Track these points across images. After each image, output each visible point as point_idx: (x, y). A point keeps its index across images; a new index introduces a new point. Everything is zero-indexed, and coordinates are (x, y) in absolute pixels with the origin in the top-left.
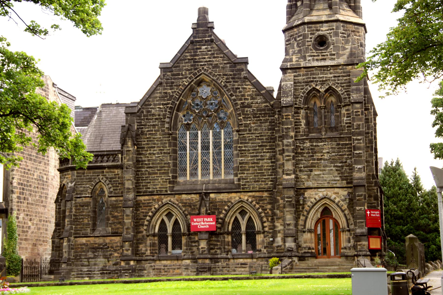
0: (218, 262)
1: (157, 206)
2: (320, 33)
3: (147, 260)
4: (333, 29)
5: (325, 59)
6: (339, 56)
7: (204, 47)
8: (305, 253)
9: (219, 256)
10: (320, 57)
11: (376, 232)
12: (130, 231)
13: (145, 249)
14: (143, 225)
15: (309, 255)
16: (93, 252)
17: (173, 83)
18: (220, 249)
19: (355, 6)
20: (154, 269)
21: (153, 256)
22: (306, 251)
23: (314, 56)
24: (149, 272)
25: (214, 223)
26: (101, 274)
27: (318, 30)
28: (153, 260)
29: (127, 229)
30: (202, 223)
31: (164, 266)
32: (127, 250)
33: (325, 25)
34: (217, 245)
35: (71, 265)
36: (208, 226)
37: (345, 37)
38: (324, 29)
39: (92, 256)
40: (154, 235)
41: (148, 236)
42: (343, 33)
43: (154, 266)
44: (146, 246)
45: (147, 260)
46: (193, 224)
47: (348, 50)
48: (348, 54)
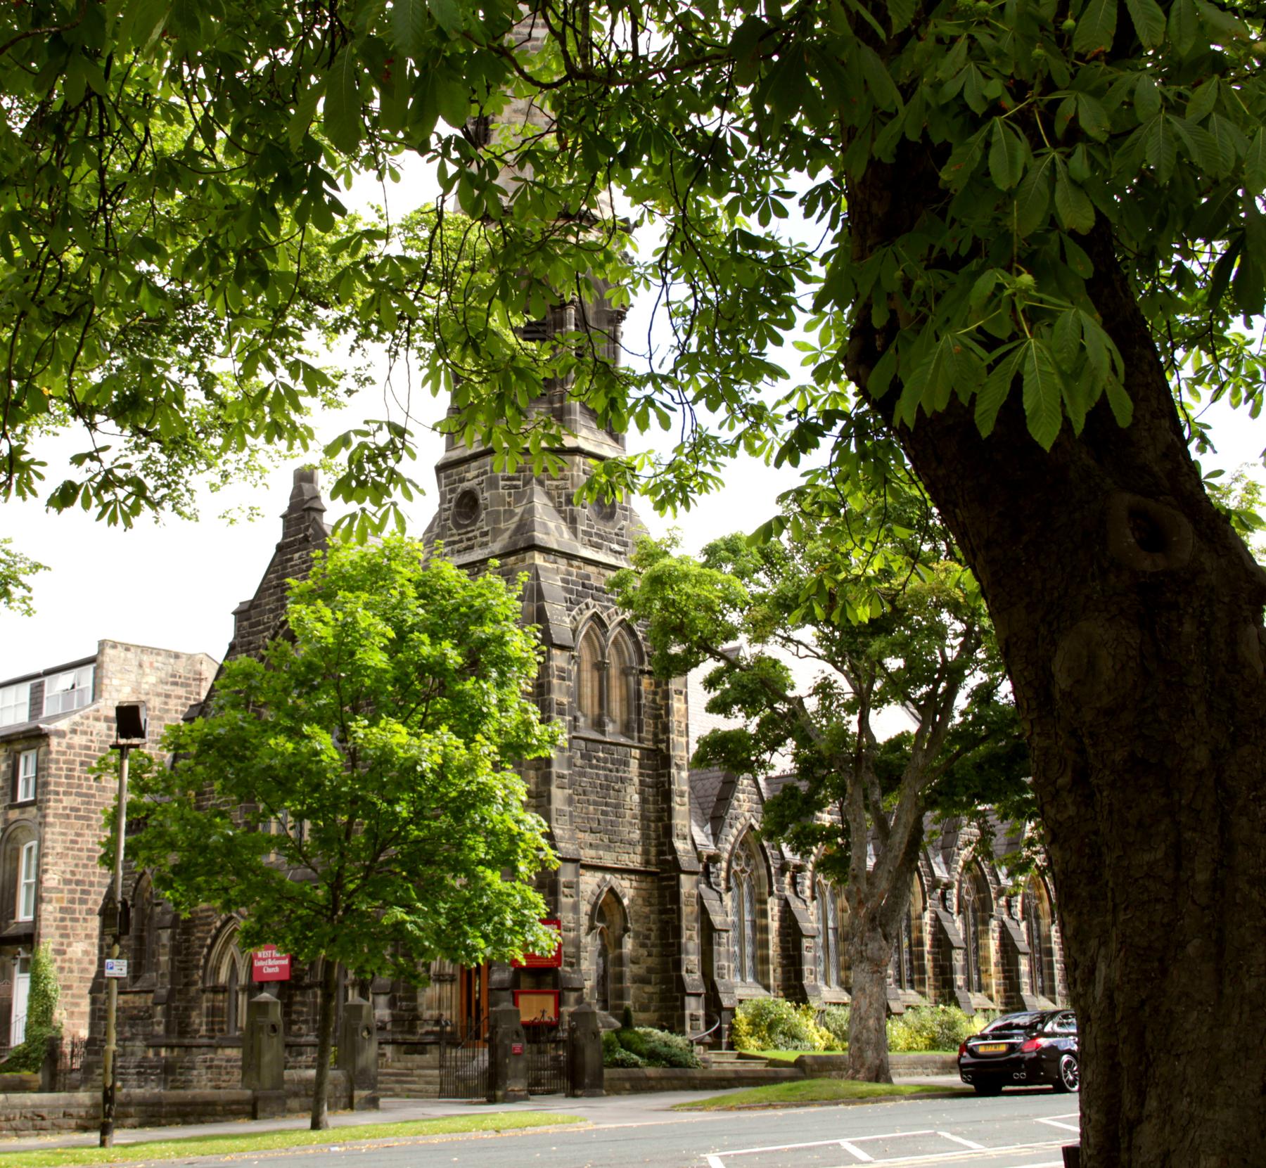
0: (301, 1054)
1: (218, 924)
2: (466, 485)
3: (199, 1047)
4: (485, 473)
5: (470, 548)
6: (497, 532)
7: (296, 556)
8: (428, 1033)
9: (303, 1040)
10: (464, 545)
11: (549, 979)
12: (167, 980)
13: (199, 1020)
14: (197, 967)
15: (431, 1038)
16: (132, 1026)
17: (250, 643)
18: (306, 1022)
19: (562, 408)
20: (209, 1067)
21: (212, 1038)
22: (429, 1028)
23: (454, 543)
24: (200, 1075)
25: (286, 962)
26: (139, 1073)
27: (462, 480)
28: (210, 1046)
29: (163, 975)
30: (270, 962)
31: (228, 1061)
32: (159, 1023)
33: (474, 464)
34: (300, 1013)
35: (97, 1053)
36: (277, 970)
37: (516, 487)
38: (469, 475)
39: (128, 1035)
40: (216, 990)
41: (204, 991)
42: (510, 479)
43: (212, 1060)
44: (200, 1015)
45: (199, 1047)
46: (257, 964)
47: (516, 519)
48: (513, 526)
